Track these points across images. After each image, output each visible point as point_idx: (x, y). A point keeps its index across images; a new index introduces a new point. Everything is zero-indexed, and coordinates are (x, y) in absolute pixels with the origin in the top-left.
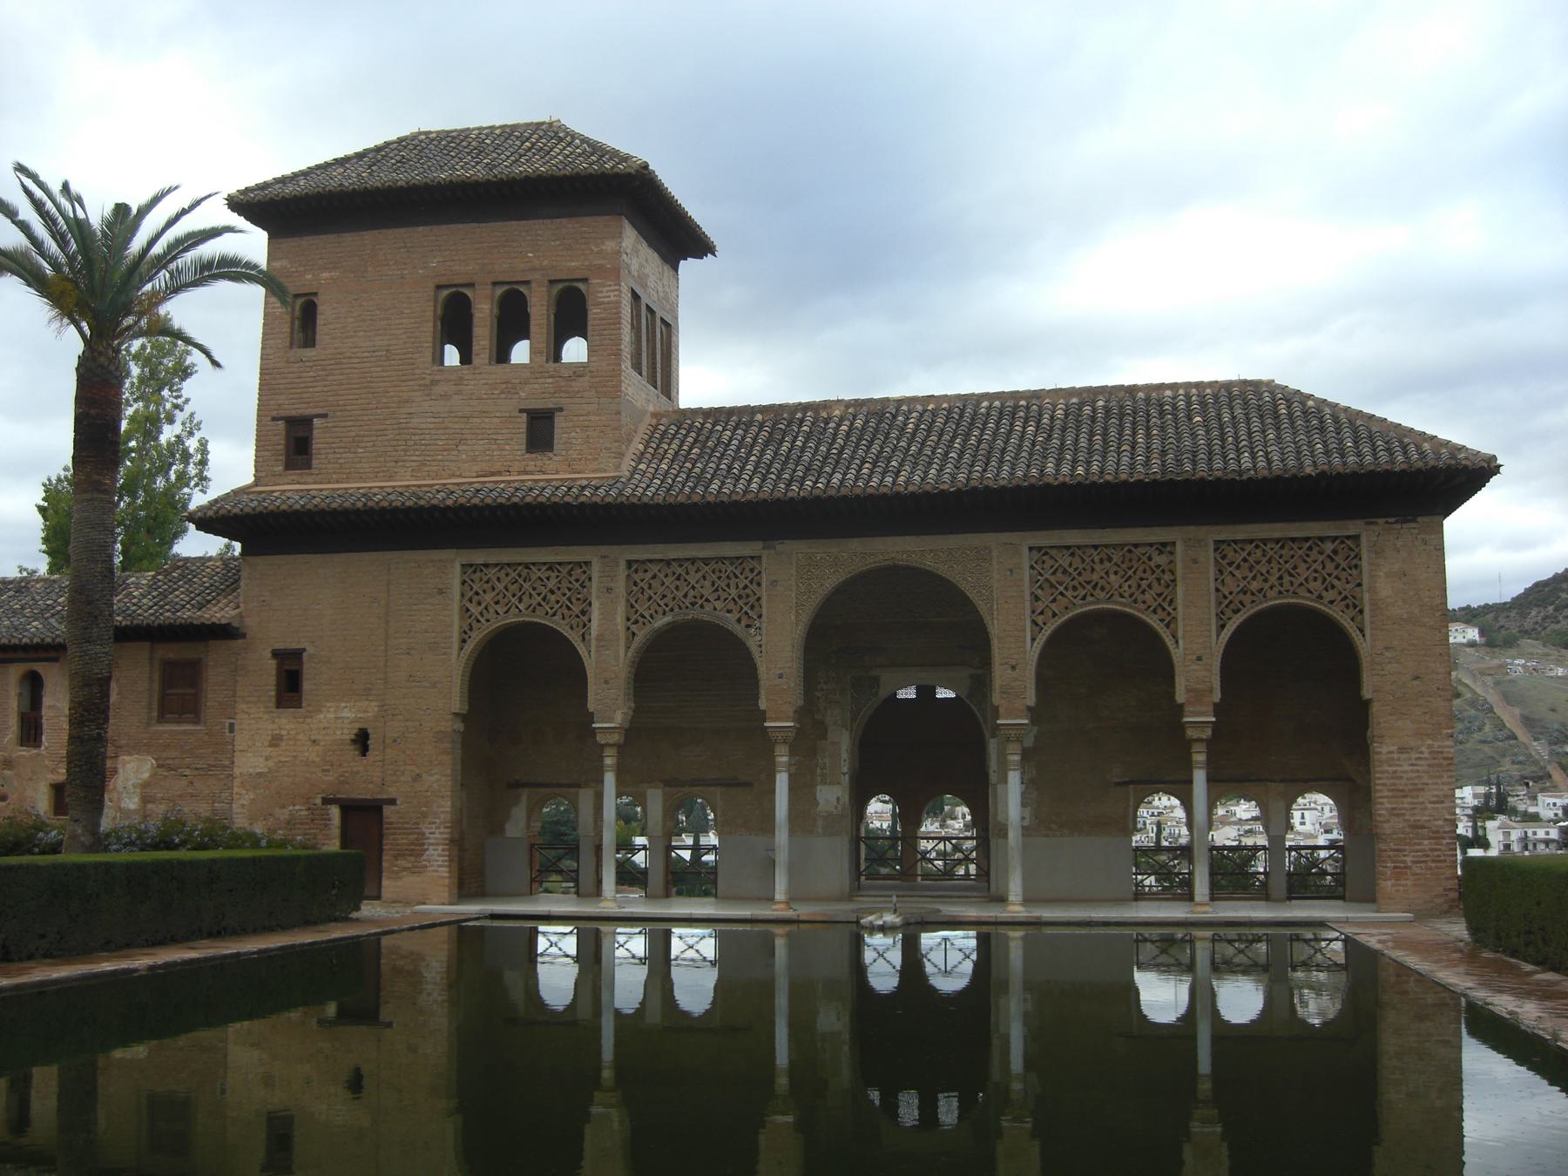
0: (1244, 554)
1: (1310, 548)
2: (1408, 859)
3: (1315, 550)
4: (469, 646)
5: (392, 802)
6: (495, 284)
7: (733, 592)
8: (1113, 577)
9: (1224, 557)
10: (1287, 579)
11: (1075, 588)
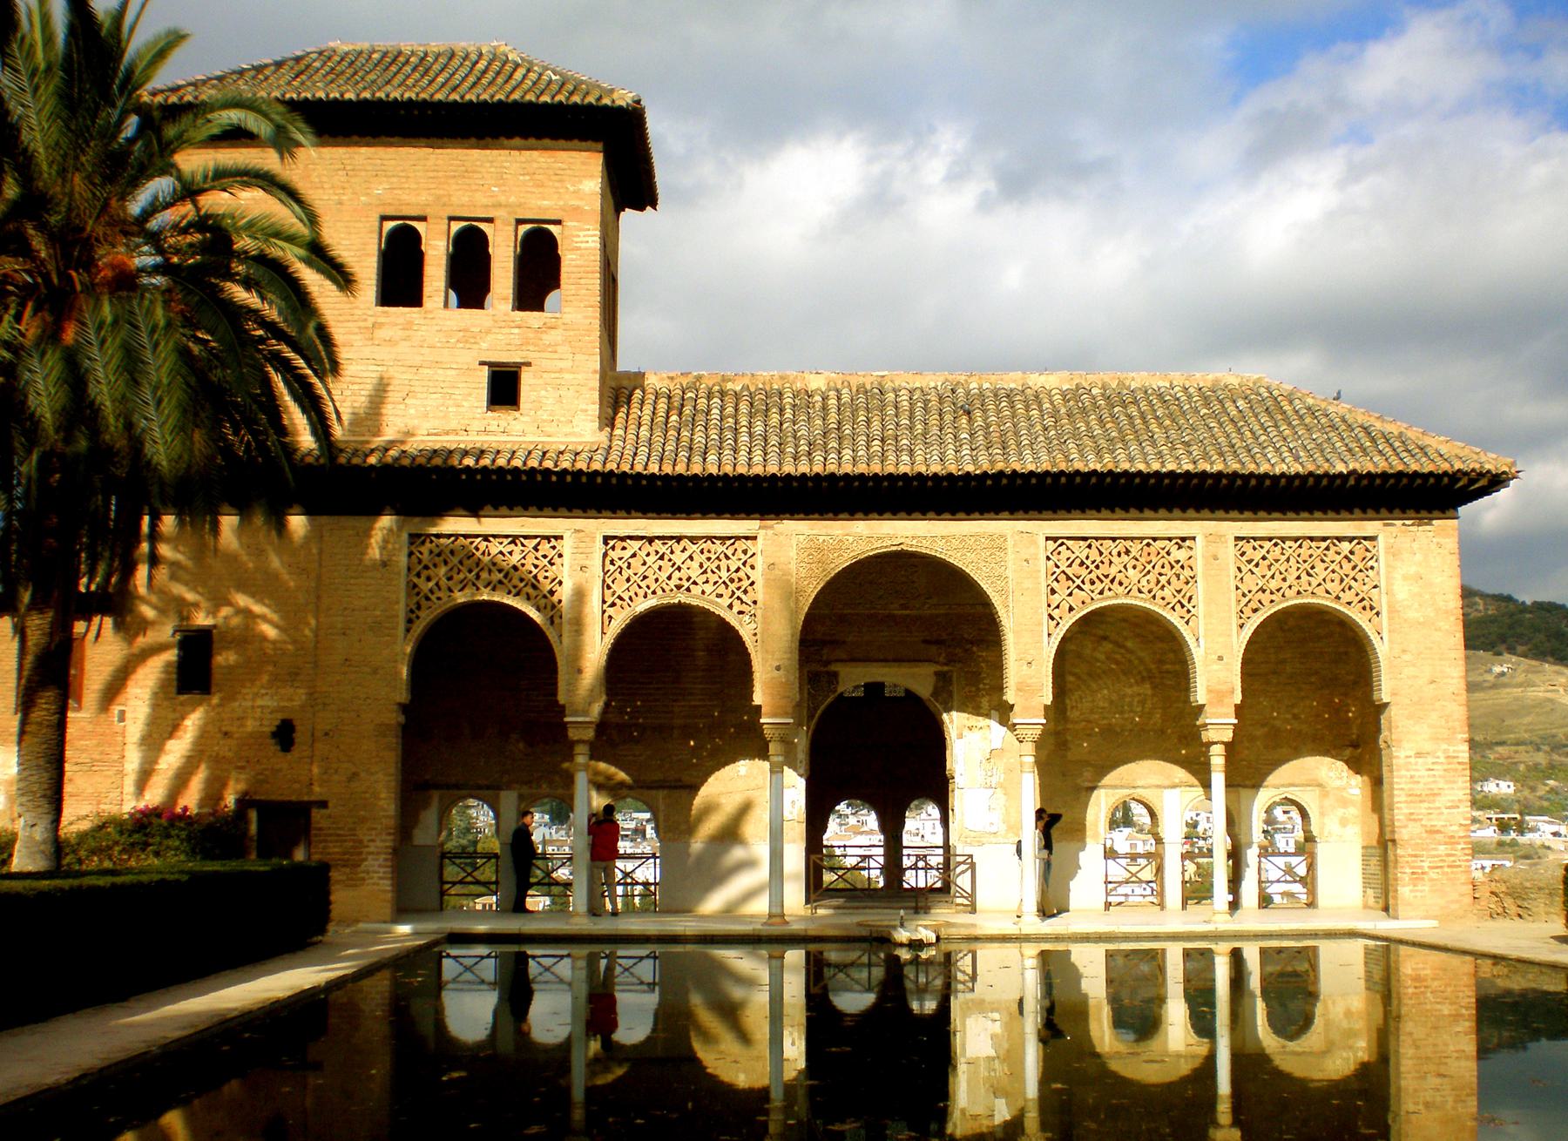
0: (1263, 552)
1: (1327, 549)
2: (1426, 864)
3: (1333, 549)
4: (419, 628)
5: (323, 804)
6: (451, 219)
7: (724, 574)
8: (1131, 571)
9: (1243, 554)
10: (1304, 577)
11: (1093, 583)
